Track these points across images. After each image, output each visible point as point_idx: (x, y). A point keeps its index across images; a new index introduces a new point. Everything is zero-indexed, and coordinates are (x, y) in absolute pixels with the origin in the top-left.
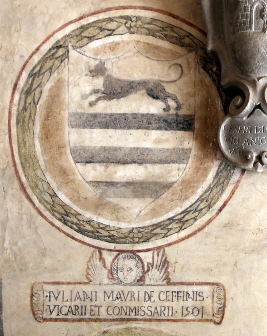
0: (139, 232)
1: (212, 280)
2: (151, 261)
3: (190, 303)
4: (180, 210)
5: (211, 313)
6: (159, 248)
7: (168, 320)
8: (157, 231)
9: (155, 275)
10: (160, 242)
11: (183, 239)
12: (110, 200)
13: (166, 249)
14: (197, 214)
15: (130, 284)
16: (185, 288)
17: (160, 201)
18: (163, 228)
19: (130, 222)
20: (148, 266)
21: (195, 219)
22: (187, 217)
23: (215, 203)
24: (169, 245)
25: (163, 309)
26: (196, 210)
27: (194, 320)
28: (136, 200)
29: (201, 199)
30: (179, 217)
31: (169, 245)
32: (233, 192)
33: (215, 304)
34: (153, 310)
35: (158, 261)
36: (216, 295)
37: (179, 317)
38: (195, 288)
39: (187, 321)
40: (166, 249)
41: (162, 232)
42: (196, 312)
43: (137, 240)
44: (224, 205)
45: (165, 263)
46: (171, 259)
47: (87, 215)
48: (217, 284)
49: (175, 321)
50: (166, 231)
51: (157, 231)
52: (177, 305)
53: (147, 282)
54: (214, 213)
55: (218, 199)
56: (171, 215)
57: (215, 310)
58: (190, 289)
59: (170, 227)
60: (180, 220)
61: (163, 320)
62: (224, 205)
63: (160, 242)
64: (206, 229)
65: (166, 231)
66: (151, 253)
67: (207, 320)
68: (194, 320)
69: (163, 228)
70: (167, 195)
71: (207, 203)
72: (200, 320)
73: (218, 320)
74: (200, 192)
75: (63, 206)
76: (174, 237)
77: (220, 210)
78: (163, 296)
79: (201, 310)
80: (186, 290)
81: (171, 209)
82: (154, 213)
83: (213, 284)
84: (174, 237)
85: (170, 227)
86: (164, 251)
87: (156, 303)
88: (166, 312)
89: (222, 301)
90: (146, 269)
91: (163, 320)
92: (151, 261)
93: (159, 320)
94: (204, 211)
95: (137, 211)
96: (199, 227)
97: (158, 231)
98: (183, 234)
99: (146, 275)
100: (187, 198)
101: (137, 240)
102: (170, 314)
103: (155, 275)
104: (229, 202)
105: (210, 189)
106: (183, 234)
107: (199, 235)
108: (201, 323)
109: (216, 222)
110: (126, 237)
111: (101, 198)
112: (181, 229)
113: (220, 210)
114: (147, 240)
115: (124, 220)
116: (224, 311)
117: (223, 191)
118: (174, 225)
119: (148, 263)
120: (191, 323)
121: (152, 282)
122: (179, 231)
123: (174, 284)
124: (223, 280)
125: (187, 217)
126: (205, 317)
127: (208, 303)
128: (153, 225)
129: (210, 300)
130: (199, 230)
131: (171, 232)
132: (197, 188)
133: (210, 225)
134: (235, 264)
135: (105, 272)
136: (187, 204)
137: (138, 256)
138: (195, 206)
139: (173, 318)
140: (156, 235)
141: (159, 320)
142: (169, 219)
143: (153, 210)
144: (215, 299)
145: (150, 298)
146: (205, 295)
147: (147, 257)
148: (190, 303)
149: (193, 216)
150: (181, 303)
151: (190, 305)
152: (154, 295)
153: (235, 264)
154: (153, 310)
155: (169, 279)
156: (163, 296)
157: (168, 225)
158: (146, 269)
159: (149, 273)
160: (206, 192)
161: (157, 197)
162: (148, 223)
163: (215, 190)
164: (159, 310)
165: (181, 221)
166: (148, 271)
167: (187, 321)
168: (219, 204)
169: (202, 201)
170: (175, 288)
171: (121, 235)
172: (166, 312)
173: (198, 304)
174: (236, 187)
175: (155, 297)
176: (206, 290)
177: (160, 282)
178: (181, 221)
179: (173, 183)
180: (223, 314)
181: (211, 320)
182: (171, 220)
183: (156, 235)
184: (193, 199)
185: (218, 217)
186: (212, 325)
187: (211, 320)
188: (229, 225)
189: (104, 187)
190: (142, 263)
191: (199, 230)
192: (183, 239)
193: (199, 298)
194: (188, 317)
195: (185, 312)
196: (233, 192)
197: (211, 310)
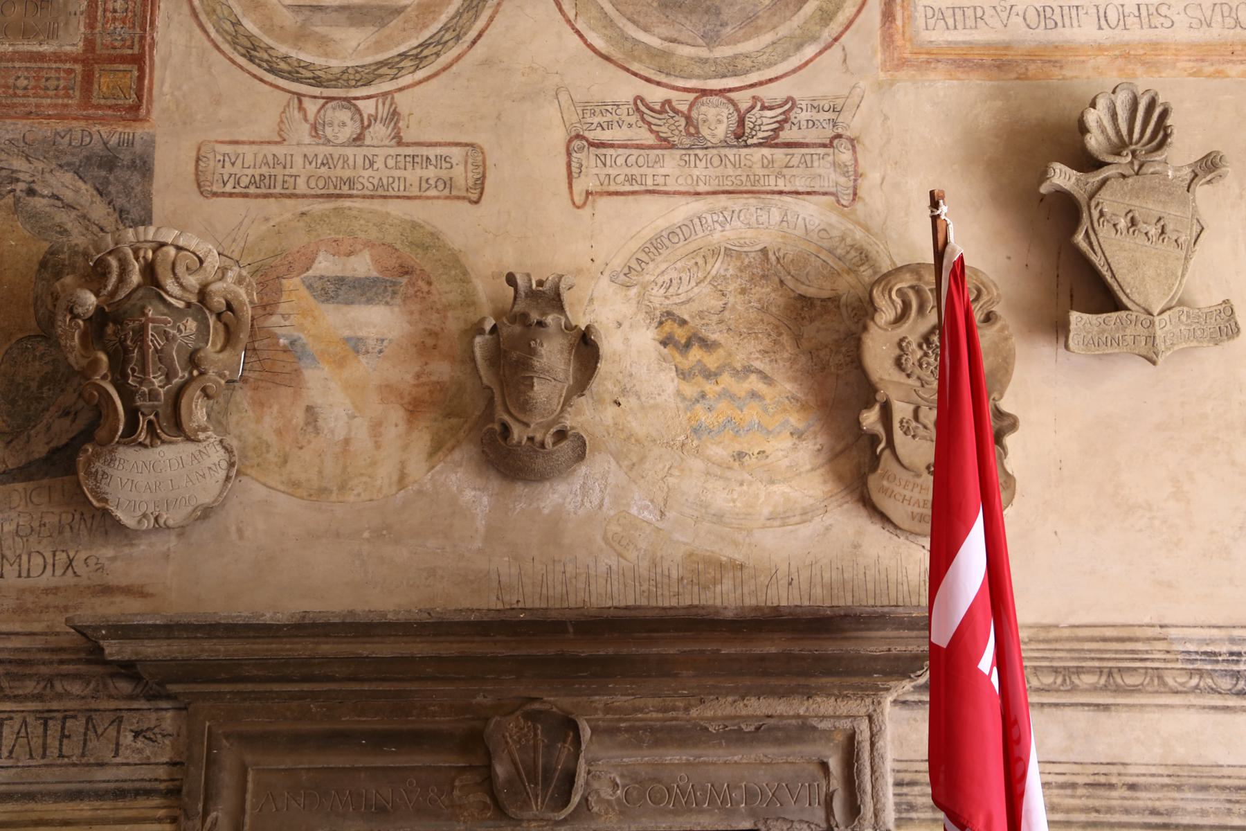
0: (357, 72)
1: (464, 140)
2: (373, 112)
3: (431, 172)
4: (415, 43)
5: (464, 187)
6: (385, 95)
7: (398, 197)
8: (381, 71)
9: (379, 131)
10: (386, 86)
11: (420, 82)
12: (317, 29)
13: (396, 95)
14: (440, 47)
15: (342, 145)
16: (425, 151)
17: (387, 31)
18: (393, 66)
19: (344, 58)
20: (369, 120)
21: (438, 55)
22: (426, 52)
23: (465, 34)
24: (401, 89)
25: (391, 180)
26: (438, 43)
27: (438, 198)
28: (352, 30)
29: (445, 28)
30: (414, 52)
31: (401, 89)
32: (491, 19)
33: (470, 175)
34: (376, 182)
35: (383, 111)
36: (470, 161)
37: (415, 191)
38: (439, 151)
39: (428, 198)
40: (396, 95)
41: (389, 71)
42: (441, 186)
43: (353, 83)
44: (480, 36)
45: (394, 115)
46: (403, 110)
47: (283, 49)
48: (472, 145)
49: (408, 198)
50: (395, 71)
51: (381, 71)
52: (413, 175)
53: (368, 141)
54: (465, 46)
55: (470, 28)
56: (402, 49)
57: (470, 183)
58: (431, 152)
59: (402, 65)
60: (416, 56)
61: (391, 197)
62: (480, 36)
63: (386, 86)
64: (454, 68)
65: (395, 71)
66: (373, 101)
67: (458, 198)
68: (438, 198)
69: (393, 66)
70: (396, 22)
71: (455, 34)
72: (447, 198)
73: (474, 197)
74: (443, 18)
75: (249, 37)
76: (407, 80)
77: (474, 42)
78: (391, 163)
79: (449, 183)
80: (425, 154)
81: (403, 41)
82: (379, 46)
83: (467, 145)
84: (407, 80)
85: (402, 65)
86: (393, 98)
87: (380, 172)
88: (395, 185)
89: (481, 170)
90: (366, 123)
91: (391, 197)
92: (373, 112)
93: (385, 197)
94: (450, 44)
95: (354, 44)
96: (443, 65)
97: (384, 70)
98: (420, 74)
99: (366, 133)
100: (425, 26)
101: (353, 83)
102: (402, 188)
103: (379, 131)
104: (487, 32)
105: (458, 14)
106: (420, 74)
107: (443, 75)
108: (448, 202)
109: (468, 58)
110: (337, 79)
111: (303, 26)
112: (417, 68)
113: (474, 42)
114: (368, 83)
115: (335, 56)
116: (483, 183)
117: (477, 17)
118: (407, 63)
119: (370, 116)
120: (435, 201)
121: (375, 142)
122: (414, 71)
123: (408, 145)
124: (480, 139)
125: (426, 52)
126: (454, 193)
127: (458, 172)
128: (376, 63)
129: (462, 168)
130: (444, 69)
131: (403, 72)
132: (440, 13)
133: (460, 62)
134: (498, 117)
135: (307, 126)
136: (426, 34)
137: (355, 106)
138: (437, 38)
139: (406, 194)
140: (381, 76)
141: (385, 197)
142: (400, 55)
143: (377, 42)
144: (470, 167)
145: (371, 165)
146: (454, 161)
147: (368, 107)
148: (431, 172)
149: (435, 50)
150: (419, 172)
151: (431, 175)
152: (378, 161)
153: (498, 117)
154: (376, 182)
155: (401, 138)
156: (391, 163)
157: (398, 63)
158: (366, 123)
159: (371, 129)
160: (452, 18)
161: (383, 26)
162: (369, 60)
163: (465, 16)
164: (385, 182)
165: (418, 58)
166: (369, 126)
167: (428, 198)
168: (473, 34)
169: (447, 31)
170: (410, 151)
171: (330, 76)
172: (395, 185)
173: (444, 174)
174: (496, 12)
175: (379, 164)
176: (456, 153)
177: (386, 142)
178: (418, 58)
179: (406, 7)
180: (483, 189)
181: (464, 198)
182: (403, 56)
183: (381, 76)
184: (434, 28)
185: (471, 52)
186: (465, 205)
187: (464, 198)
188: (486, 63)
189: (308, 13)
190: (361, 115)
191: (444, 69)
192: (420, 82)
193: (444, 165)
194: (429, 193)
195: (424, 185)
196: (491, 19)
197: (463, 182)
